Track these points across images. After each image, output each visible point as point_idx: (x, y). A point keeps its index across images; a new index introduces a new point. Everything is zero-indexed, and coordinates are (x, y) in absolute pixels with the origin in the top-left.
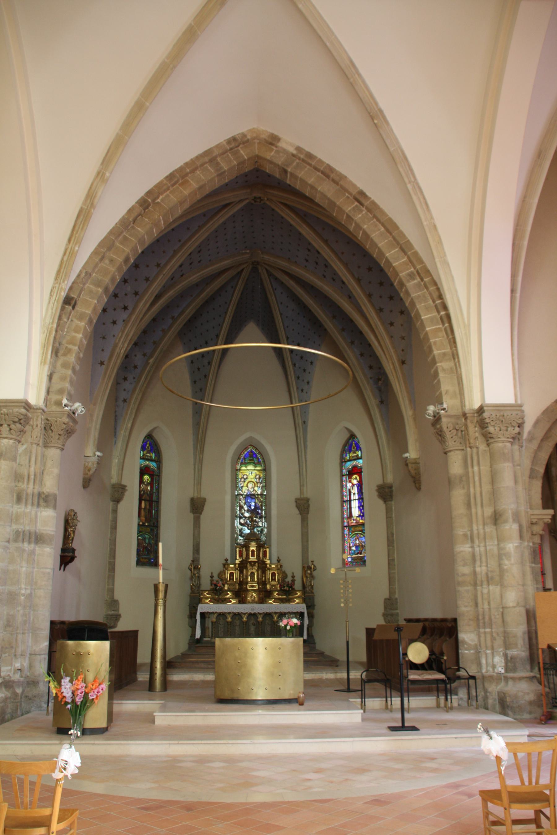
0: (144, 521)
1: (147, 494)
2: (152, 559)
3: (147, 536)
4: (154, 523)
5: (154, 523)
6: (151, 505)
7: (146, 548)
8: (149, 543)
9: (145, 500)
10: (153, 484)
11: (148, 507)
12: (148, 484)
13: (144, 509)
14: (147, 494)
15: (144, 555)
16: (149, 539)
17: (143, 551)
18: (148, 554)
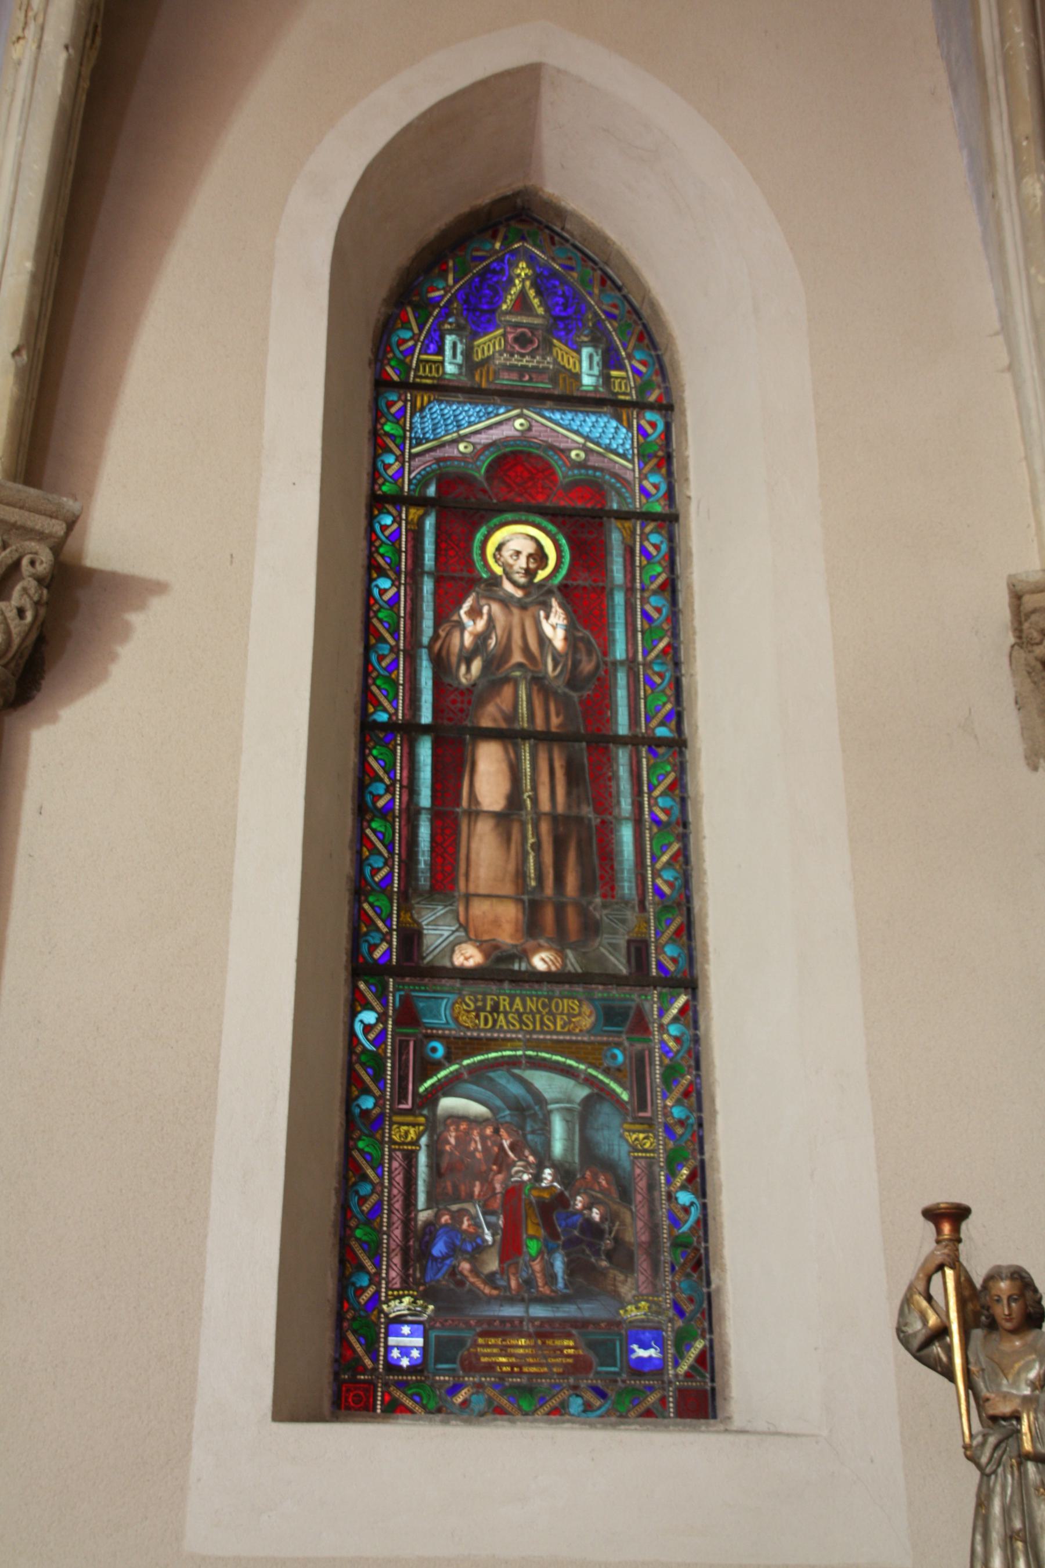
0: (507, 937)
1: (538, 681)
2: (640, 1334)
3: (545, 1083)
4: (638, 950)
5: (638, 950)
6: (588, 777)
7: (551, 1209)
8: (588, 1151)
9: (507, 735)
10: (601, 593)
11: (549, 794)
12: (536, 596)
13: (507, 818)
14: (538, 681)
15: (528, 1294)
16: (584, 1116)
17: (511, 1246)
18: (584, 1278)
